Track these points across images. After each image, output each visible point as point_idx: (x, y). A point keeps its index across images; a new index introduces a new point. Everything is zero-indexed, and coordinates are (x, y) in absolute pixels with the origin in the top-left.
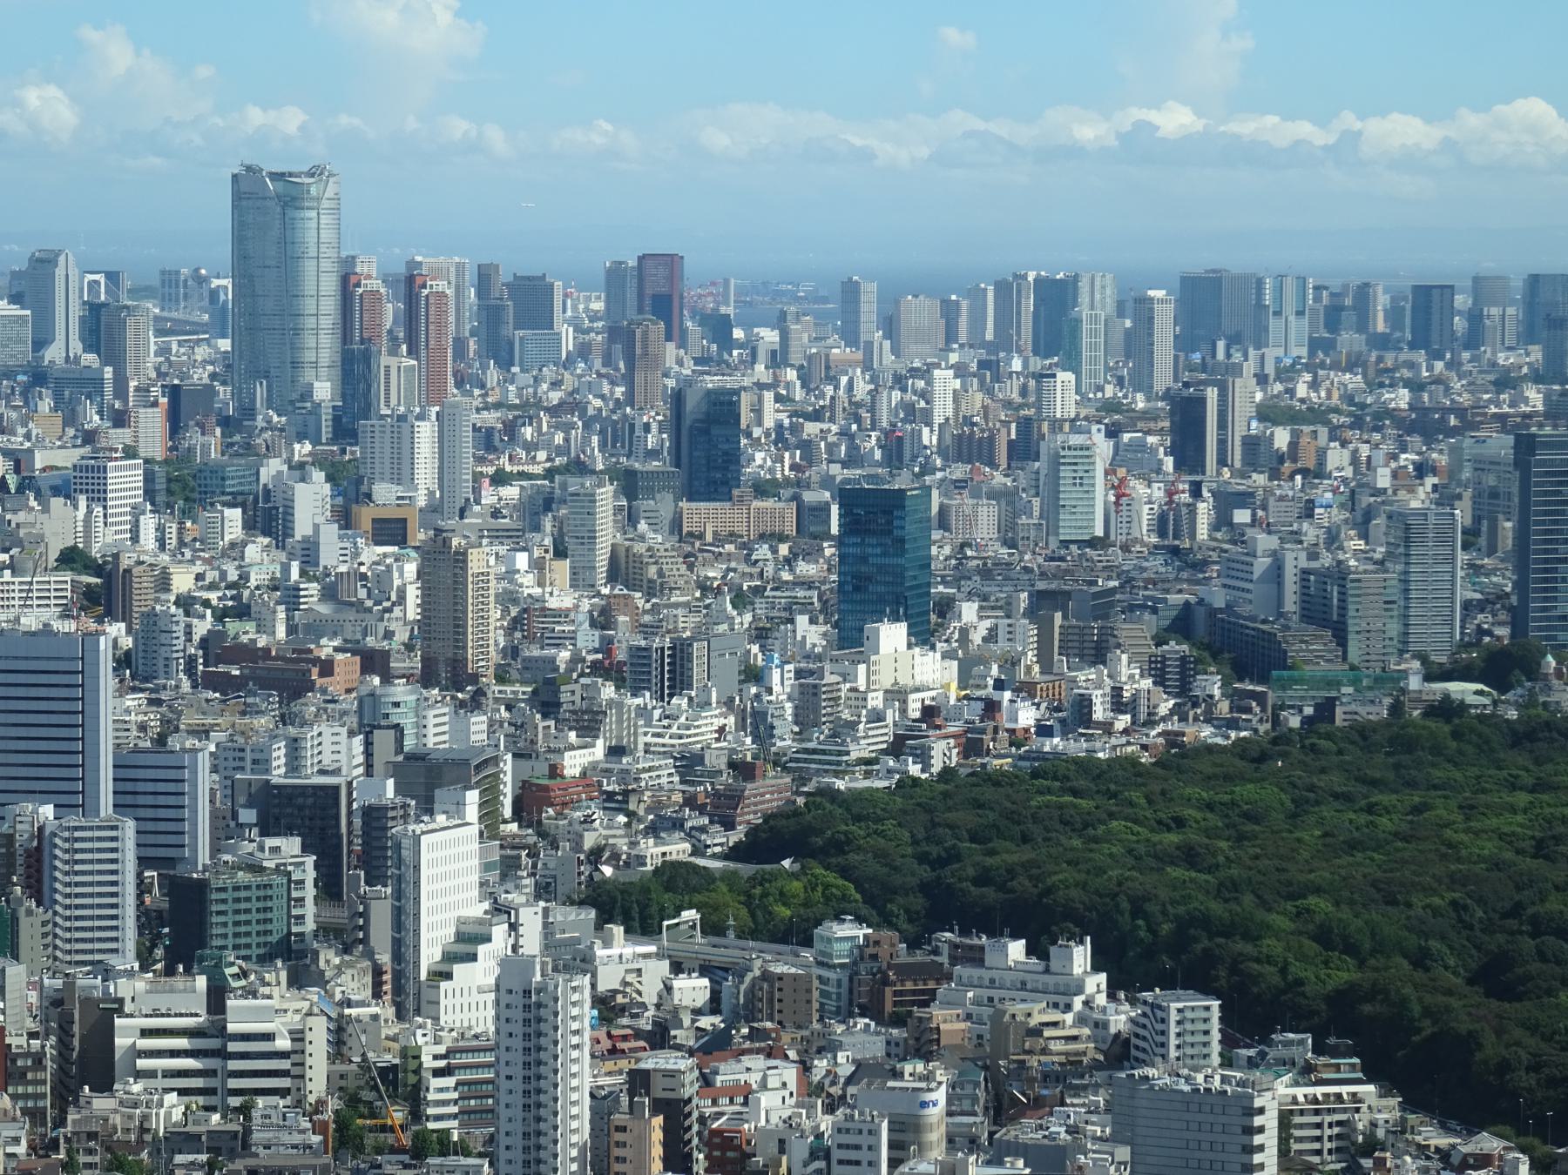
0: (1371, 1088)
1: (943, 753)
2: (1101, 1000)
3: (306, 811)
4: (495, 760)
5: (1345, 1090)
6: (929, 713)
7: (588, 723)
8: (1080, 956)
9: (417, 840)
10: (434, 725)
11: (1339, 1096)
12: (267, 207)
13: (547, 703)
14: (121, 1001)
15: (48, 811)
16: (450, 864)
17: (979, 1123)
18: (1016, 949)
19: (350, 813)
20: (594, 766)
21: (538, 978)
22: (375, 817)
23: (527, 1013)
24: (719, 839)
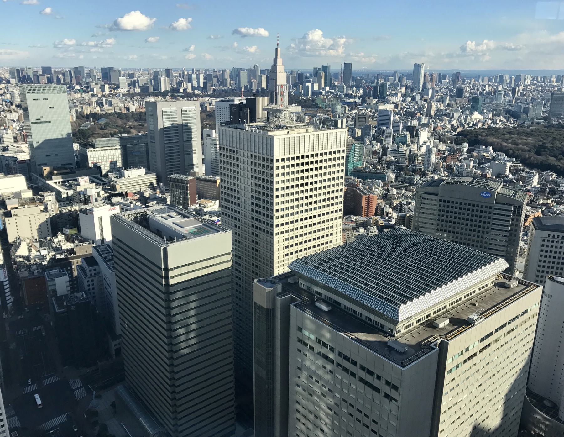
1: (480, 125)
3: (410, 129)
7: (442, 121)
8: (491, 148)
10: (425, 120)
12: (418, 67)
15: (385, 128)
16: (424, 135)
18: (484, 147)
23: (429, 150)
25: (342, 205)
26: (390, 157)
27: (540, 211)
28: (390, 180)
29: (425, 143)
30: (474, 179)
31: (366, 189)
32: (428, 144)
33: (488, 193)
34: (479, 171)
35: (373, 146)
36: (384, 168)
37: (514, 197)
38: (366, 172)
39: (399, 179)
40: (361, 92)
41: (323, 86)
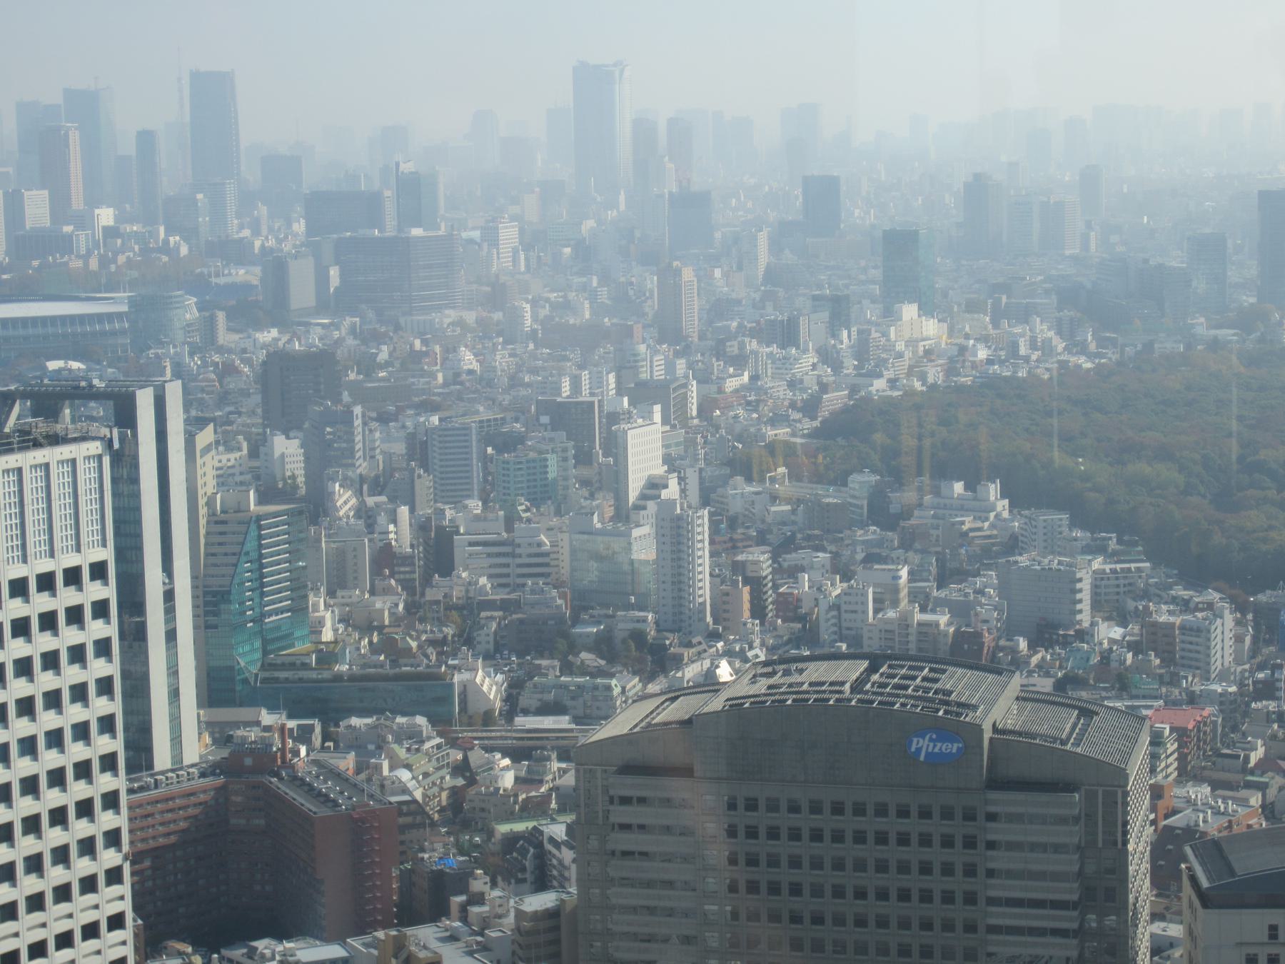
0: (1148, 564)
1: (935, 374)
2: (1006, 514)
3: (572, 420)
4: (685, 386)
5: (1133, 566)
6: (928, 352)
7: (739, 361)
9: (625, 432)
10: (654, 366)
11: (1129, 569)
12: (594, 83)
13: (719, 352)
14: (457, 527)
17: (930, 585)
19: (600, 417)
20: (743, 387)
21: (678, 511)
22: (613, 418)
24: (808, 425)
25: (125, 889)
26: (473, 577)
27: (1255, 800)
28: (476, 707)
29: (654, 486)
30: (873, 669)
31: (337, 775)
32: (672, 491)
33: (945, 731)
34: (943, 619)
35: (370, 527)
36: (438, 643)
37: (1077, 744)
38: (338, 678)
39: (526, 699)
40: (300, 227)
41: (78, 203)
